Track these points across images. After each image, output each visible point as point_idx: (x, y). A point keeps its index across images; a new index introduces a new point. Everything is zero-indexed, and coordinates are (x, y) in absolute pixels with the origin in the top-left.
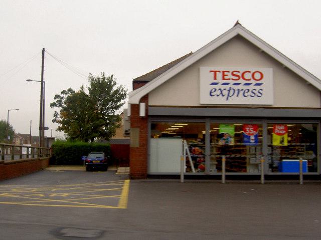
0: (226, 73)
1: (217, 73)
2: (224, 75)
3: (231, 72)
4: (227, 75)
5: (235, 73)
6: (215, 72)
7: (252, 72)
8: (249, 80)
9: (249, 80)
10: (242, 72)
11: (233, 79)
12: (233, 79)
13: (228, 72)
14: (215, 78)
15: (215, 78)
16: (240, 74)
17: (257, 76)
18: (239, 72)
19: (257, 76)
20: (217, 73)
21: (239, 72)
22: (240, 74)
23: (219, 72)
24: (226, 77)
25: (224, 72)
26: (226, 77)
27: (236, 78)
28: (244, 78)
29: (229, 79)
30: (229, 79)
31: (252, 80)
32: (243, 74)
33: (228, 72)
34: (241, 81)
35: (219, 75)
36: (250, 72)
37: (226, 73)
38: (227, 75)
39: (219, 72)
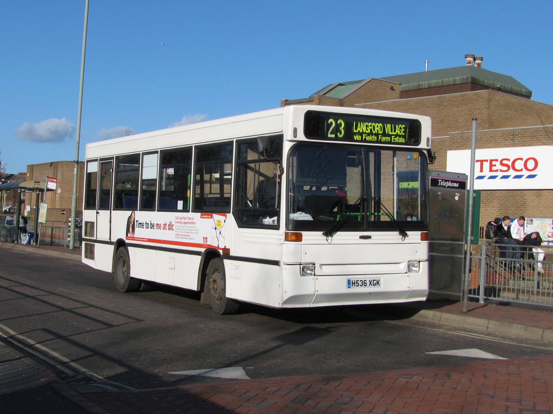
0: (494, 163)
1: (484, 163)
2: (491, 165)
3: (499, 161)
4: (495, 165)
5: (504, 162)
6: (482, 162)
7: (524, 160)
8: (521, 170)
9: (521, 170)
10: (511, 161)
11: (501, 171)
12: (501, 171)
13: (497, 160)
14: (481, 170)
15: (481, 170)
16: (510, 163)
17: (531, 164)
18: (509, 160)
19: (531, 164)
20: (484, 163)
21: (509, 160)
22: (510, 163)
23: (487, 161)
24: (494, 168)
25: (491, 161)
26: (494, 168)
27: (506, 168)
28: (515, 169)
29: (497, 171)
30: (497, 171)
31: (524, 169)
33: (497, 160)
34: (512, 173)
35: (486, 165)
36: (521, 159)
37: (494, 163)
38: (495, 165)
39: (487, 161)
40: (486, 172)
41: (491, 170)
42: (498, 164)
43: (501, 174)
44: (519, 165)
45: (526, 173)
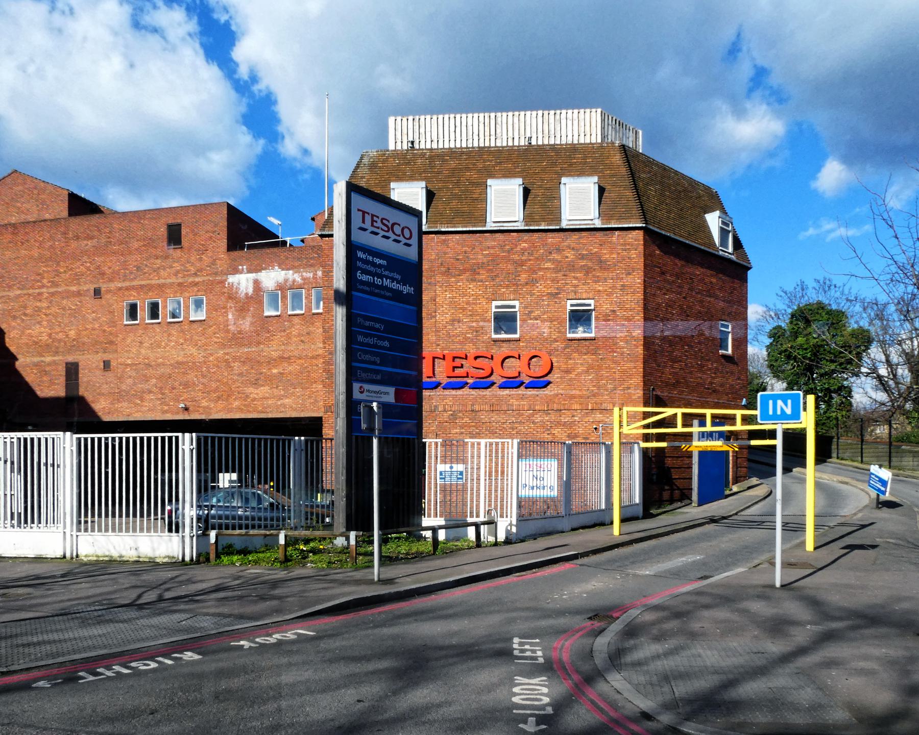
0: (375, 218)
2: (373, 221)
4: (376, 222)
5: (384, 221)
6: (364, 213)
9: (399, 236)
10: (391, 222)
11: (382, 229)
12: (382, 229)
14: (364, 222)
15: (364, 222)
18: (388, 221)
21: (388, 221)
23: (368, 214)
24: (375, 224)
29: (378, 228)
30: (378, 228)
32: (393, 224)
33: (378, 217)
34: (390, 234)
38: (376, 222)
39: (368, 214)
40: (368, 224)
41: (372, 225)
42: (379, 221)
43: (382, 233)
44: (397, 229)
45: (401, 238)
